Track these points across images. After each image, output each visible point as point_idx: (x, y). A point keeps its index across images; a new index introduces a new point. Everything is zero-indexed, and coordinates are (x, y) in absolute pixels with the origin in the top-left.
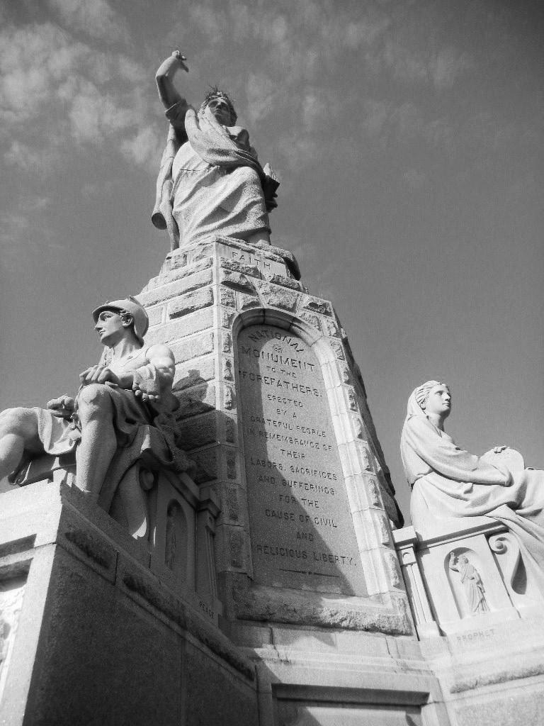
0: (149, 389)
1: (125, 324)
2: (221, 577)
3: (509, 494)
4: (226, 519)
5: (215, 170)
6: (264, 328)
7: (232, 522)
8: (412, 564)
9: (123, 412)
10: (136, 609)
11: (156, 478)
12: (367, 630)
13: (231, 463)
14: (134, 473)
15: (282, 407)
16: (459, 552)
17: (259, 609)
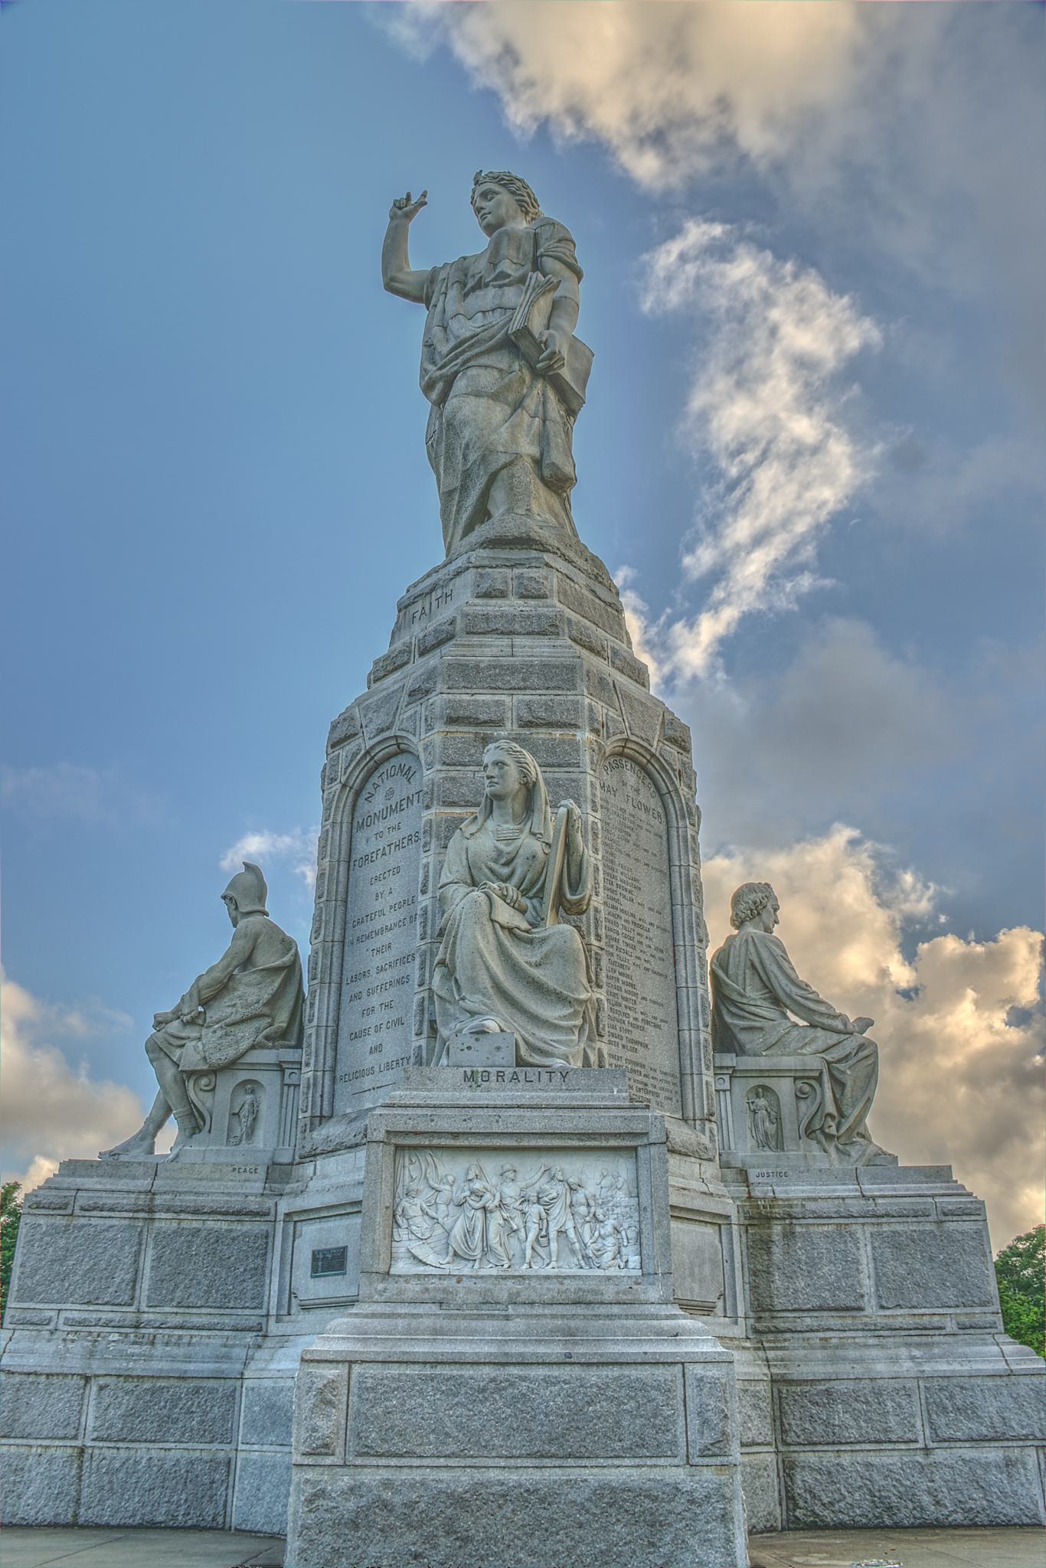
10: (93, 1221)
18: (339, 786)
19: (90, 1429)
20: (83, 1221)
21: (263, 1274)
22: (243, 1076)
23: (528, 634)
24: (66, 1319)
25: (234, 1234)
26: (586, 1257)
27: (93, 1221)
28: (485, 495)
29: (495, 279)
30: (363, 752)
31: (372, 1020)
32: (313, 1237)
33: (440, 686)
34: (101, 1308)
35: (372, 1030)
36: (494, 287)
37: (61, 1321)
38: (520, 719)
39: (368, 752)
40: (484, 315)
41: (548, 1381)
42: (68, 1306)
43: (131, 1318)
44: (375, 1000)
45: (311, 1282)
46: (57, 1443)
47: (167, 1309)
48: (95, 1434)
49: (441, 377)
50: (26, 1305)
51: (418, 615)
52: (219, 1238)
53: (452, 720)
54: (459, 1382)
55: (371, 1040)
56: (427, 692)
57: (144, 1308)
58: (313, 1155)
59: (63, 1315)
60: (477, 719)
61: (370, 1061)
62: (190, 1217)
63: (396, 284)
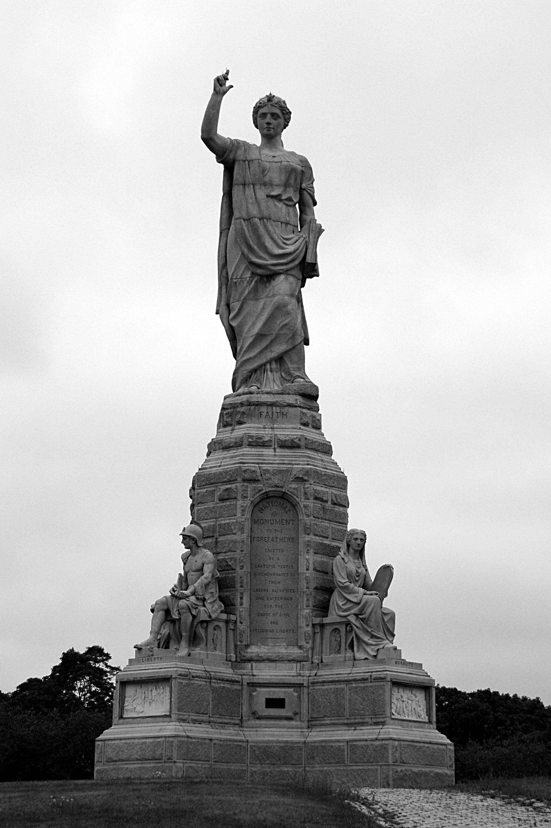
0: (201, 594)
1: (193, 542)
2: (236, 646)
3: (355, 610)
4: (238, 624)
5: (256, 282)
6: (268, 500)
7: (241, 625)
8: (318, 633)
9: (192, 607)
11: (207, 625)
12: (290, 661)
13: (241, 598)
14: (199, 625)
15: (271, 555)
16: (336, 630)
17: (248, 656)
18: (250, 502)
19: (212, 758)
20: (193, 682)
21: (240, 705)
22: (216, 623)
23: (322, 452)
24: (192, 719)
25: (233, 689)
26: (419, 716)
27: (197, 682)
28: (286, 352)
29: (286, 200)
30: (264, 491)
31: (269, 611)
32: (264, 693)
33: (312, 481)
34: (200, 715)
35: (272, 614)
36: (285, 204)
37: (190, 719)
38: (332, 500)
39: (266, 492)
40: (281, 224)
41: (428, 747)
42: (191, 714)
43: (208, 719)
44: (272, 603)
45: (266, 709)
46: (205, 763)
47: (217, 716)
48: (214, 760)
49: (272, 270)
50: (180, 713)
51: (264, 414)
52: (229, 690)
53: (316, 498)
54: (416, 746)
55: (271, 618)
56: (306, 481)
57: (211, 716)
58: (250, 660)
59: (191, 717)
60: (323, 499)
61: (270, 627)
62: (220, 682)
63: (211, 142)
